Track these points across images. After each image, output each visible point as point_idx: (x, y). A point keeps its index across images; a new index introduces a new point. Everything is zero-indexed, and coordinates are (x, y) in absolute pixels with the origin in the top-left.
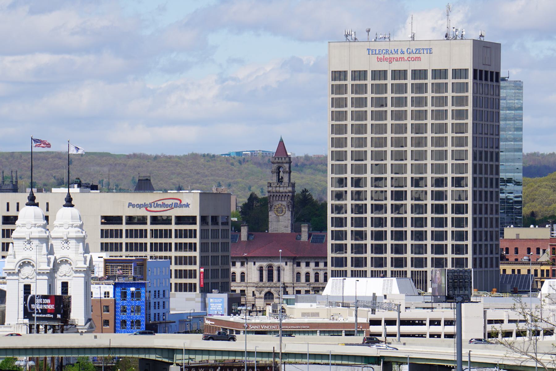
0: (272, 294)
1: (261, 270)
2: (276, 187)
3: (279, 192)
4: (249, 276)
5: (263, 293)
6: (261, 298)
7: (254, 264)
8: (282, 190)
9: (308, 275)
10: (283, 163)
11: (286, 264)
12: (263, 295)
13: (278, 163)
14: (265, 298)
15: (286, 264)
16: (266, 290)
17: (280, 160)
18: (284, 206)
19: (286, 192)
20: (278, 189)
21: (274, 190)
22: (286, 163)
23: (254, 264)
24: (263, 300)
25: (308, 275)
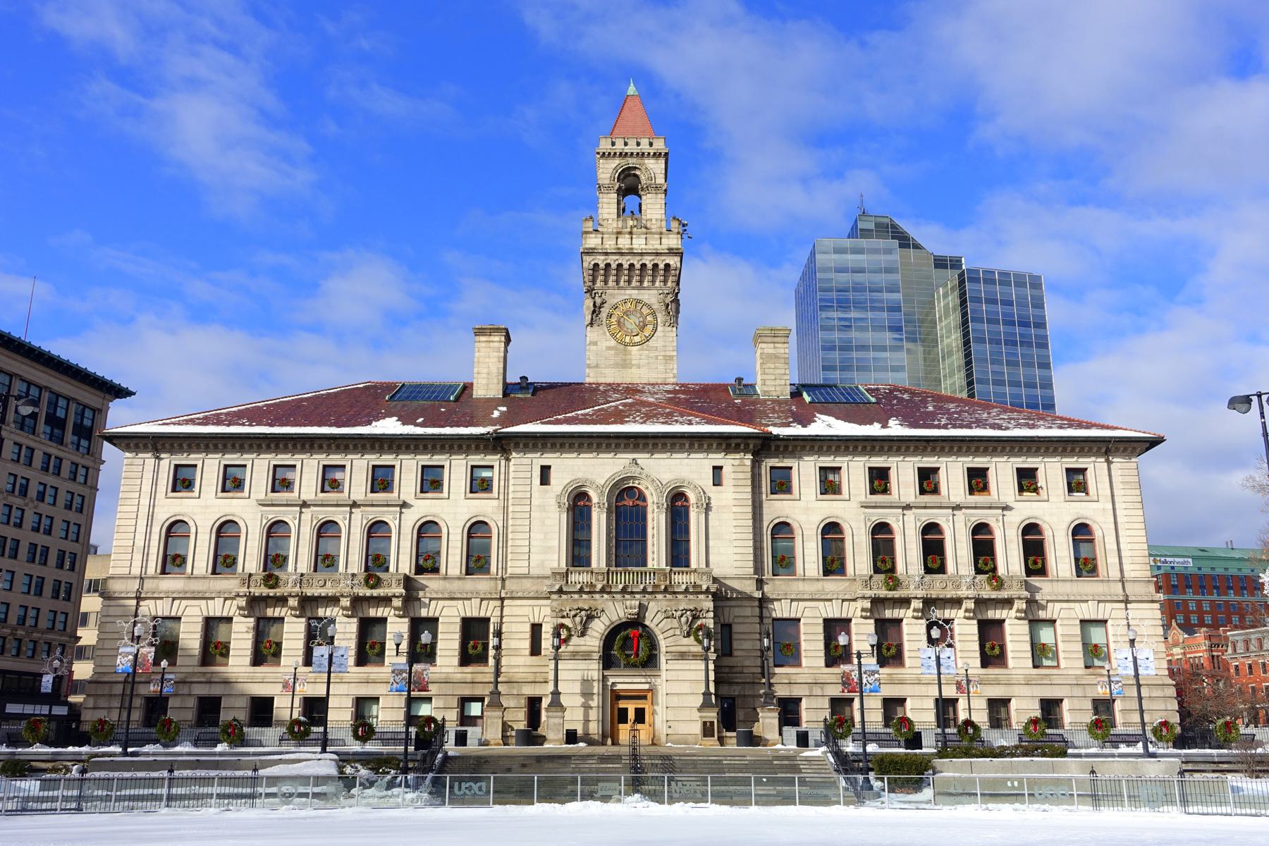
1: (578, 505)
3: (631, 253)
4: (517, 540)
5: (599, 627)
6: (586, 656)
7: (545, 480)
8: (639, 243)
9: (831, 531)
10: (642, 155)
11: (717, 482)
12: (593, 641)
13: (623, 155)
14: (608, 662)
15: (717, 482)
16: (615, 611)
17: (632, 148)
18: (649, 307)
19: (657, 254)
20: (624, 242)
21: (610, 244)
22: (657, 155)
23: (545, 480)
24: (593, 669)
25: (831, 531)
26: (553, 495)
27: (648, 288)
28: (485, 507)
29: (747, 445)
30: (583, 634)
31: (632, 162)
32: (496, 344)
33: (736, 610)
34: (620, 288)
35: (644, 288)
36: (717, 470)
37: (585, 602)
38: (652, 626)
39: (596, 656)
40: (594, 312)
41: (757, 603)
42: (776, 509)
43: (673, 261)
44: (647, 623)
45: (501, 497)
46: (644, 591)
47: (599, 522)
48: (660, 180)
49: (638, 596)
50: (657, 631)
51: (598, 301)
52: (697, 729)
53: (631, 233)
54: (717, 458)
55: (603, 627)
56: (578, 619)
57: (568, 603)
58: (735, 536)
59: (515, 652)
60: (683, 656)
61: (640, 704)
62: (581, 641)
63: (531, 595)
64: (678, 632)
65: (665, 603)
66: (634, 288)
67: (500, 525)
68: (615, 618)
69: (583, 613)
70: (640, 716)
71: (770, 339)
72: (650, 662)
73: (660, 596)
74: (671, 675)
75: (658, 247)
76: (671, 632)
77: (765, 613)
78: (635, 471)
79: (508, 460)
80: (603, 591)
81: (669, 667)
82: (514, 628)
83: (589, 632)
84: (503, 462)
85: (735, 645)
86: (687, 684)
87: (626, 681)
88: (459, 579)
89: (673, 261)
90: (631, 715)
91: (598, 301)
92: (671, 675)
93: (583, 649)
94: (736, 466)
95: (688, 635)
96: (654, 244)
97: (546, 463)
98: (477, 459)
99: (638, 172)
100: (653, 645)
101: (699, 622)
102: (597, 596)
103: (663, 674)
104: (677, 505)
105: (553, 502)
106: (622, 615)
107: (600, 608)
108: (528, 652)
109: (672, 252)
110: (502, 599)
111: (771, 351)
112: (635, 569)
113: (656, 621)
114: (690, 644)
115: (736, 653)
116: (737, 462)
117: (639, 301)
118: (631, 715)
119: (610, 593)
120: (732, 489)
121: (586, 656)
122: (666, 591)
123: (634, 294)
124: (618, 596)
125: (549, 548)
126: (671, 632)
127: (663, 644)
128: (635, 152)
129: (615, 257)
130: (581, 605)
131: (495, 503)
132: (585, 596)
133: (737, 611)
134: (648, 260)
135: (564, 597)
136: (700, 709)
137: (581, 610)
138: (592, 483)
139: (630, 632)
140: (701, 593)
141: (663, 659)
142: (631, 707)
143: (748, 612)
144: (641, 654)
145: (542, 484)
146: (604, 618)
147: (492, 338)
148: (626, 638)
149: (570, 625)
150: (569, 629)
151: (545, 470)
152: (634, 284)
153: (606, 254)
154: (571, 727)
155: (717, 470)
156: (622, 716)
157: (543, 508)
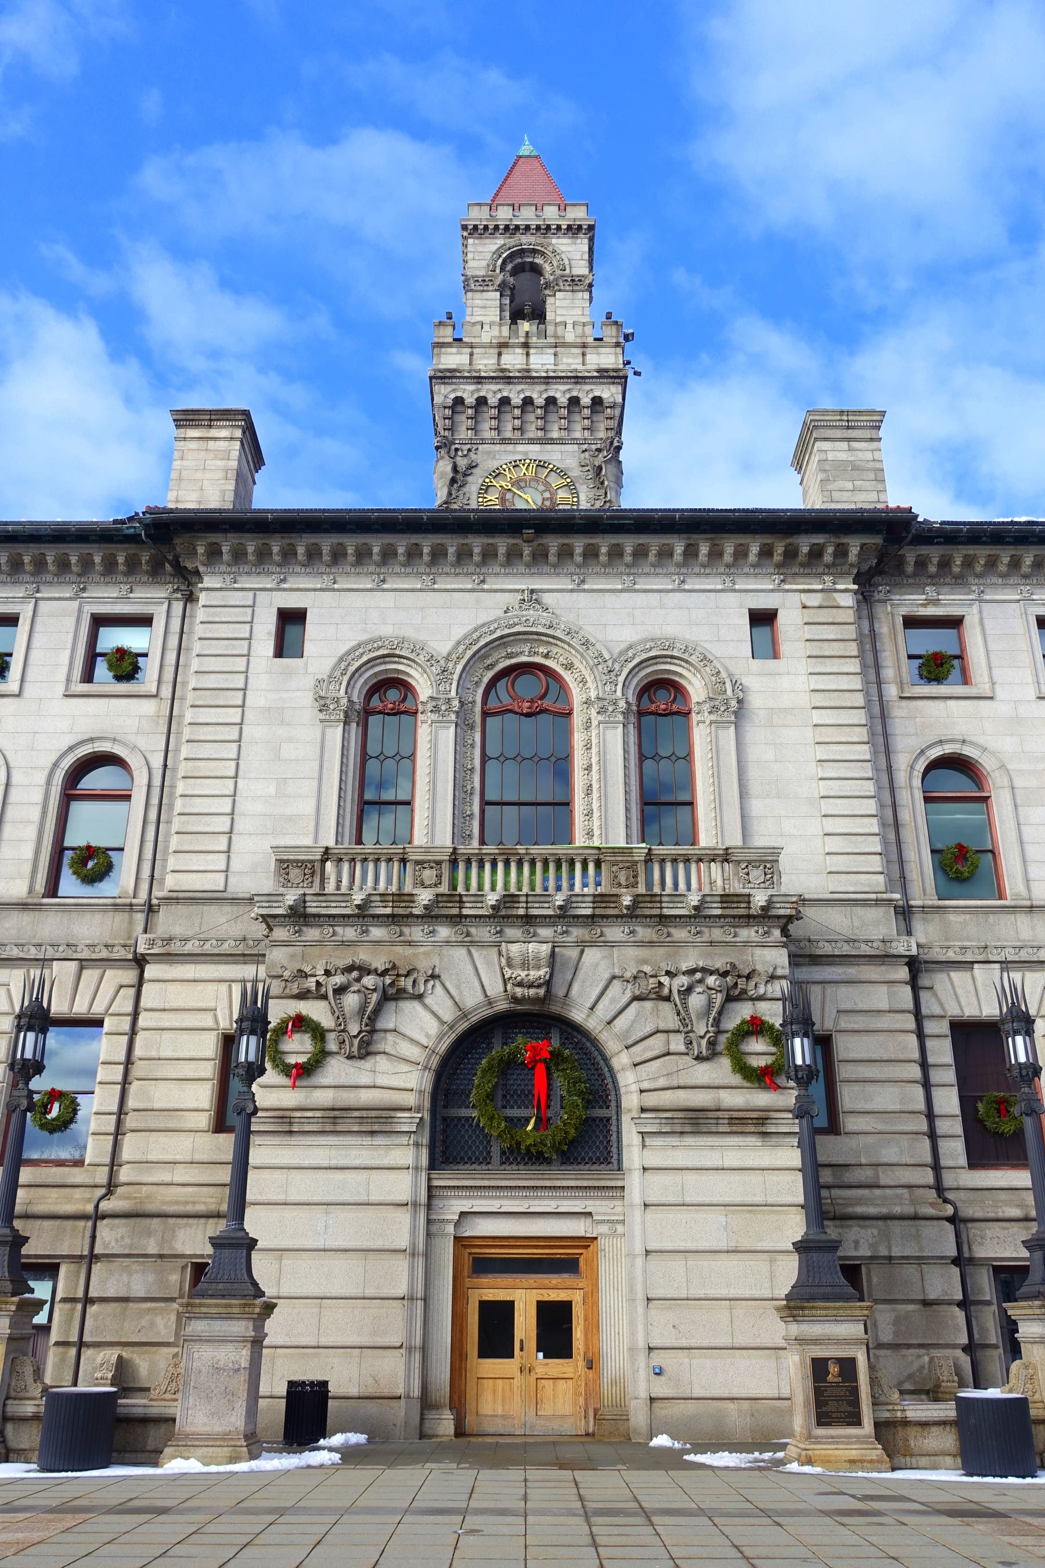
0: (583, 1063)
2: (502, 346)
3: (527, 377)
5: (420, 1030)
6: (375, 1122)
8: (541, 361)
10: (546, 230)
12: (400, 1071)
13: (510, 230)
14: (450, 1143)
16: (471, 978)
17: (527, 216)
18: (562, 473)
19: (578, 379)
20: (513, 360)
21: (485, 363)
22: (574, 230)
24: (396, 1167)
26: (309, 682)
27: (561, 441)
28: (122, 720)
29: (841, 552)
30: (365, 1049)
31: (527, 240)
32: (222, 445)
33: (843, 990)
34: (504, 441)
35: (552, 441)
36: (762, 619)
37: (377, 947)
38: (593, 1024)
39: (406, 1122)
40: (453, 481)
41: (903, 973)
42: (936, 720)
43: (609, 393)
44: (578, 1015)
45: (166, 692)
46: (564, 916)
47: (436, 752)
48: (581, 269)
49: (545, 932)
50: (610, 1043)
51: (462, 463)
52: (787, 1378)
53: (526, 345)
54: (761, 590)
55: (433, 1027)
56: (351, 1000)
57: (319, 954)
58: (824, 788)
59: (167, 1121)
60: (696, 1121)
61: (555, 1289)
62: (359, 1072)
63: (226, 948)
64: (677, 1043)
65: (632, 952)
66: (532, 441)
67: (157, 762)
68: (472, 999)
69: (369, 981)
70: (556, 1329)
71: (839, 434)
72: (585, 1142)
73: (615, 932)
74: (660, 1187)
75: (580, 367)
76: (656, 1044)
77: (929, 1005)
78: (535, 619)
79: (190, 598)
80: (430, 916)
81: (653, 1159)
82: (168, 1046)
83: (388, 1043)
84: (178, 607)
85: (848, 1097)
86: (717, 1217)
87: (509, 1210)
88: (23, 906)
89: (609, 393)
90: (525, 1325)
91: (462, 463)
92: (660, 1187)
93: (366, 1097)
94: (813, 609)
95: (711, 1055)
96: (571, 362)
97: (292, 601)
98: (108, 598)
99: (539, 260)
100: (597, 1089)
101: (744, 1011)
102: (416, 933)
103: (635, 1184)
104: (657, 700)
105: (306, 699)
106: (495, 988)
107: (424, 966)
108: (204, 1120)
109: (605, 375)
110: (140, 962)
111: (843, 456)
112: (535, 850)
113: (605, 1010)
114: (716, 1083)
115: (850, 1123)
116: (814, 600)
117: (541, 465)
118: (525, 1325)
119: (457, 920)
120: (804, 666)
121: (375, 1122)
122: (632, 915)
123: (534, 451)
124: (483, 933)
125: (290, 819)
126: (656, 1044)
127: (631, 1084)
128: (533, 223)
129: (494, 387)
130: (363, 956)
131: (148, 707)
132: (377, 933)
133: (846, 997)
134: (561, 393)
135: (312, 934)
136: (798, 1303)
137: (364, 970)
138: (418, 648)
139: (522, 1044)
140: (749, 919)
141: (630, 1135)
142: (525, 1298)
143: (879, 998)
144: (560, 1116)
145: (279, 653)
146: (437, 999)
147: (214, 433)
148: (507, 1066)
149: (327, 1021)
150: (318, 1033)
151: (291, 620)
152: (532, 433)
153: (479, 380)
154: (308, 1372)
155: (762, 619)
156: (495, 1331)
157: (276, 715)
